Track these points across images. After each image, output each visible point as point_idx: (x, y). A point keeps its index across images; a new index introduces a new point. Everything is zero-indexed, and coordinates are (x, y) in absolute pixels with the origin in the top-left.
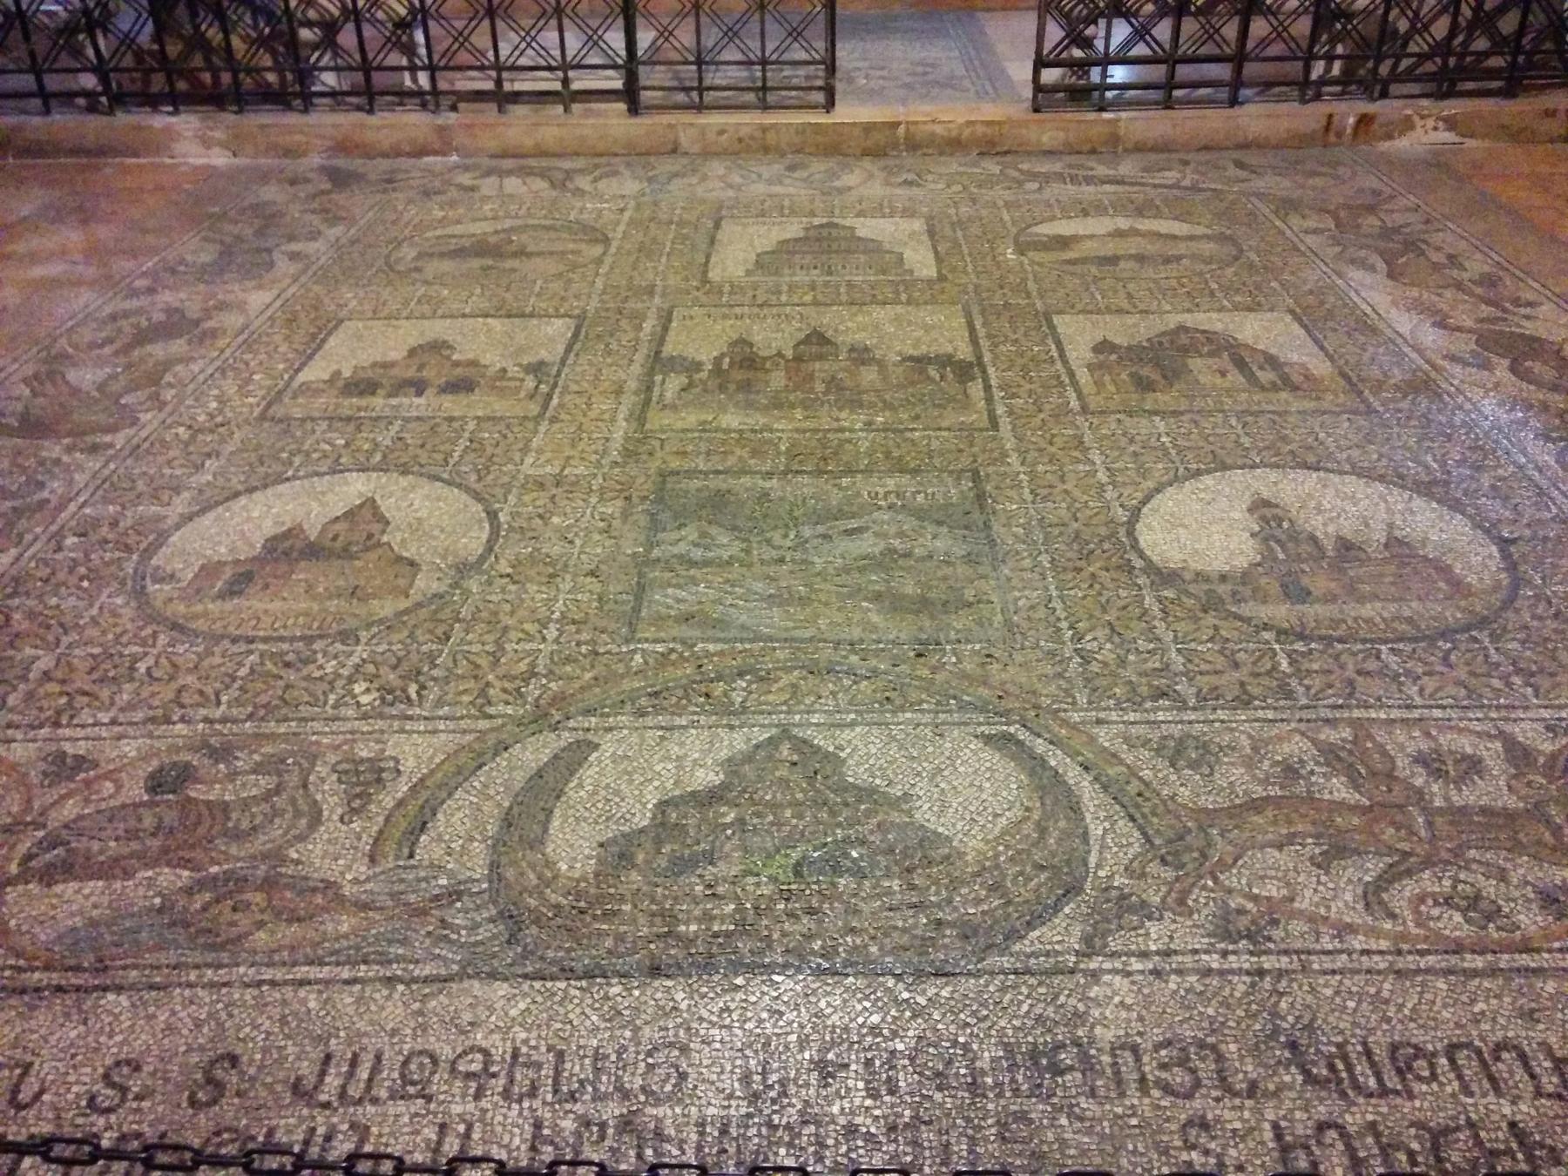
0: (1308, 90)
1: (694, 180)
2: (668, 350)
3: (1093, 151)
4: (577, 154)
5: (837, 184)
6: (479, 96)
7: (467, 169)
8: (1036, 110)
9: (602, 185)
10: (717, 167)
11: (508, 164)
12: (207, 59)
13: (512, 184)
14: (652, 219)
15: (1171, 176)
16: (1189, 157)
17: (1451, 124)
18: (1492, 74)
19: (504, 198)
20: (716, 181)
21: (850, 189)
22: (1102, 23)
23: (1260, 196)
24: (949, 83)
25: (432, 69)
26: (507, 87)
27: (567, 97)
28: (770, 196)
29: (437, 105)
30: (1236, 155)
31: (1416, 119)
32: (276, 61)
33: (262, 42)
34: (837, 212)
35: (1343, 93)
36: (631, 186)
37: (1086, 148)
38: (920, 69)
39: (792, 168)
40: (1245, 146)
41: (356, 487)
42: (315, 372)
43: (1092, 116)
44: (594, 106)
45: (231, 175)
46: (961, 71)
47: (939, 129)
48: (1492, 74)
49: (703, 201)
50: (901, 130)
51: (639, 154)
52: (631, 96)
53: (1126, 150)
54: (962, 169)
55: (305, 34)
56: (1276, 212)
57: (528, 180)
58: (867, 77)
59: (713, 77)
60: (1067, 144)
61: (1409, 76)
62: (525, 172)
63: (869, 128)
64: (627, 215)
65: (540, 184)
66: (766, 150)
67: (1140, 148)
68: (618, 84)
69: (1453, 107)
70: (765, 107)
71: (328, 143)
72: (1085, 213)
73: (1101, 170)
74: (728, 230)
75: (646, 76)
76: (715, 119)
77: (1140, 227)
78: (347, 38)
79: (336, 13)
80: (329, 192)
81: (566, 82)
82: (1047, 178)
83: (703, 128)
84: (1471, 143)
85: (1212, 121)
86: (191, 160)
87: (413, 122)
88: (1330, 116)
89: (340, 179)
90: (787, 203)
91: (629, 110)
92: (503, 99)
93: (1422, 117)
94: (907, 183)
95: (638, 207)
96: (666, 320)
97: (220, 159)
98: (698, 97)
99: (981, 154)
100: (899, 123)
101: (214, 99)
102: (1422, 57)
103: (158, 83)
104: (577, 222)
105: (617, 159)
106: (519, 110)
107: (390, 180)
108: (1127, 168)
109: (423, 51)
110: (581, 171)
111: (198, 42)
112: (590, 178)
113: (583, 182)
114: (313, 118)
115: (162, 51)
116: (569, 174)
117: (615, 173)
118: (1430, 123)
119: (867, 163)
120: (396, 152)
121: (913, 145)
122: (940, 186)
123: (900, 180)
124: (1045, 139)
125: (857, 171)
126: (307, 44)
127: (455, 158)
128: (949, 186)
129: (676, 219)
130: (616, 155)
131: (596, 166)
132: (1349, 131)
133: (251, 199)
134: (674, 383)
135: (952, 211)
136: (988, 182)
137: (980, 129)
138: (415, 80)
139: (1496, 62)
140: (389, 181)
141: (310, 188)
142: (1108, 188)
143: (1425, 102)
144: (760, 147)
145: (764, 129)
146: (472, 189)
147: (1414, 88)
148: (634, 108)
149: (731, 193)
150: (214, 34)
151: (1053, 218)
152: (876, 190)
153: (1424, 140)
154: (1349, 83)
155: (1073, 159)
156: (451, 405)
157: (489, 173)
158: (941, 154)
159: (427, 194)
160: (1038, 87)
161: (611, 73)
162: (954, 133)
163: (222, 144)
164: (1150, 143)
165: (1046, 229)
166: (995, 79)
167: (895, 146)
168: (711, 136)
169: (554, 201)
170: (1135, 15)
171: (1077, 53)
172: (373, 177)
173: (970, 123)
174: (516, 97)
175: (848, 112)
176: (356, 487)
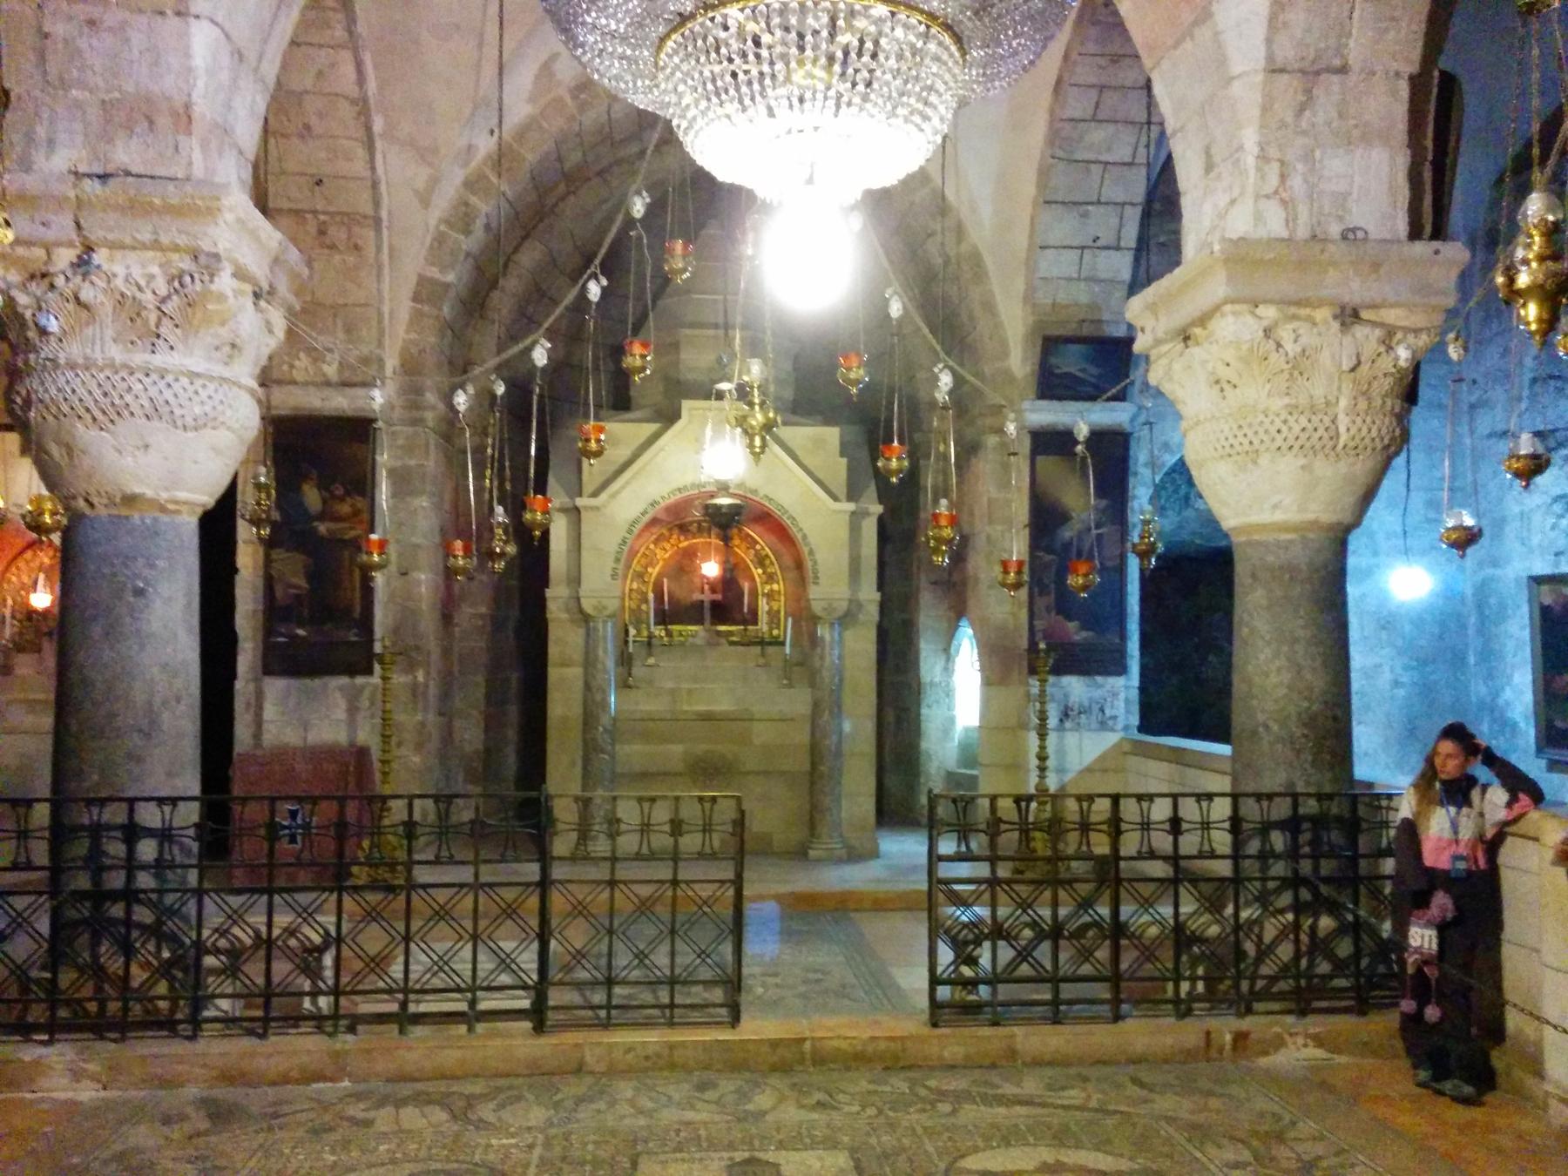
0: (1183, 1009)
1: (602, 1105)
3: (993, 1066)
4: (477, 1076)
5: (750, 1107)
6: (381, 1018)
7: (358, 1097)
8: (935, 1025)
9: (506, 1114)
10: (625, 1089)
11: (406, 1090)
12: (99, 989)
13: (411, 1117)
14: (564, 1159)
15: (1074, 1095)
16: (1084, 1071)
17: (1319, 1041)
18: (1339, 993)
19: (403, 1134)
21: (765, 1113)
22: (987, 945)
23: (1170, 1120)
24: (842, 992)
25: (336, 992)
26: (412, 1008)
27: (472, 1017)
28: (688, 1123)
29: (336, 1026)
30: (1131, 1069)
31: (1286, 1037)
32: (172, 988)
33: (165, 970)
34: (757, 1143)
35: (1212, 1008)
36: (537, 1115)
37: (987, 1062)
38: (811, 976)
39: (702, 1087)
40: (1136, 1061)
43: (987, 1031)
44: (500, 1025)
45: (96, 1111)
46: (851, 979)
47: (844, 1045)
48: (1339, 993)
49: (613, 1133)
50: (807, 1046)
51: (543, 1076)
52: (538, 1016)
53: (1024, 1064)
54: (871, 1087)
56: (1189, 1140)
57: (428, 1109)
58: (764, 985)
60: (967, 1057)
61: (1265, 995)
62: (422, 1100)
63: (775, 1044)
64: (537, 1152)
65: (440, 1115)
66: (672, 1066)
67: (1037, 1063)
68: (525, 1004)
70: (671, 1024)
71: (215, 1073)
72: (1006, 1142)
73: (1009, 1089)
75: (555, 997)
76: (622, 1037)
77: (1066, 1160)
78: (254, 970)
79: (248, 942)
80: (206, 1133)
81: (473, 1003)
82: (959, 1098)
83: (611, 1046)
84: (1342, 1059)
85: (1102, 1037)
86: (55, 1095)
87: (303, 1046)
88: (1208, 1033)
89: (220, 1115)
90: (702, 1132)
91: (534, 1029)
92: (405, 1020)
93: (1291, 1035)
94: (820, 1105)
95: (548, 1145)
97: (87, 1093)
98: (608, 1017)
99: (886, 1069)
100: (804, 1040)
102: (1273, 979)
103: (37, 1014)
104: (484, 1164)
105: (521, 1080)
106: (418, 1031)
107: (274, 1116)
108: (1031, 1085)
109: (329, 974)
110: (484, 1097)
111: (98, 971)
112: (492, 1105)
113: (486, 1111)
114: (200, 1046)
115: (54, 981)
116: (471, 1101)
117: (519, 1098)
118: (1300, 1040)
119: (774, 1080)
120: (285, 1080)
121: (821, 1059)
122: (856, 1108)
123: (812, 1100)
124: (946, 1054)
125: (768, 1091)
126: (213, 971)
127: (346, 1083)
128: (863, 1108)
129: (589, 1157)
130: (518, 1076)
131: (499, 1090)
132: (1228, 1047)
133: (118, 1147)
135: (873, 1141)
136: (899, 1104)
137: (882, 1045)
138: (314, 1003)
139: (1341, 983)
140: (276, 1116)
141: (187, 1127)
142: (1020, 1110)
143: (1290, 1019)
144: (668, 1063)
145: (672, 1047)
146: (368, 1123)
147: (1276, 1006)
148: (540, 1028)
149: (642, 1121)
150: (115, 965)
151: (976, 1150)
152: (792, 1114)
153: (1297, 1055)
154: (1213, 999)
155: (977, 1074)
157: (382, 1103)
158: (848, 1069)
159: (316, 1132)
160: (935, 1004)
161: (521, 993)
162: (859, 1048)
163: (94, 1078)
164: (1047, 1057)
166: (885, 992)
167: (802, 1061)
168: (618, 1054)
169: (457, 1136)
170: (1016, 938)
171: (967, 971)
172: (254, 1109)
173: (873, 1039)
174: (419, 1019)
175: (757, 1027)
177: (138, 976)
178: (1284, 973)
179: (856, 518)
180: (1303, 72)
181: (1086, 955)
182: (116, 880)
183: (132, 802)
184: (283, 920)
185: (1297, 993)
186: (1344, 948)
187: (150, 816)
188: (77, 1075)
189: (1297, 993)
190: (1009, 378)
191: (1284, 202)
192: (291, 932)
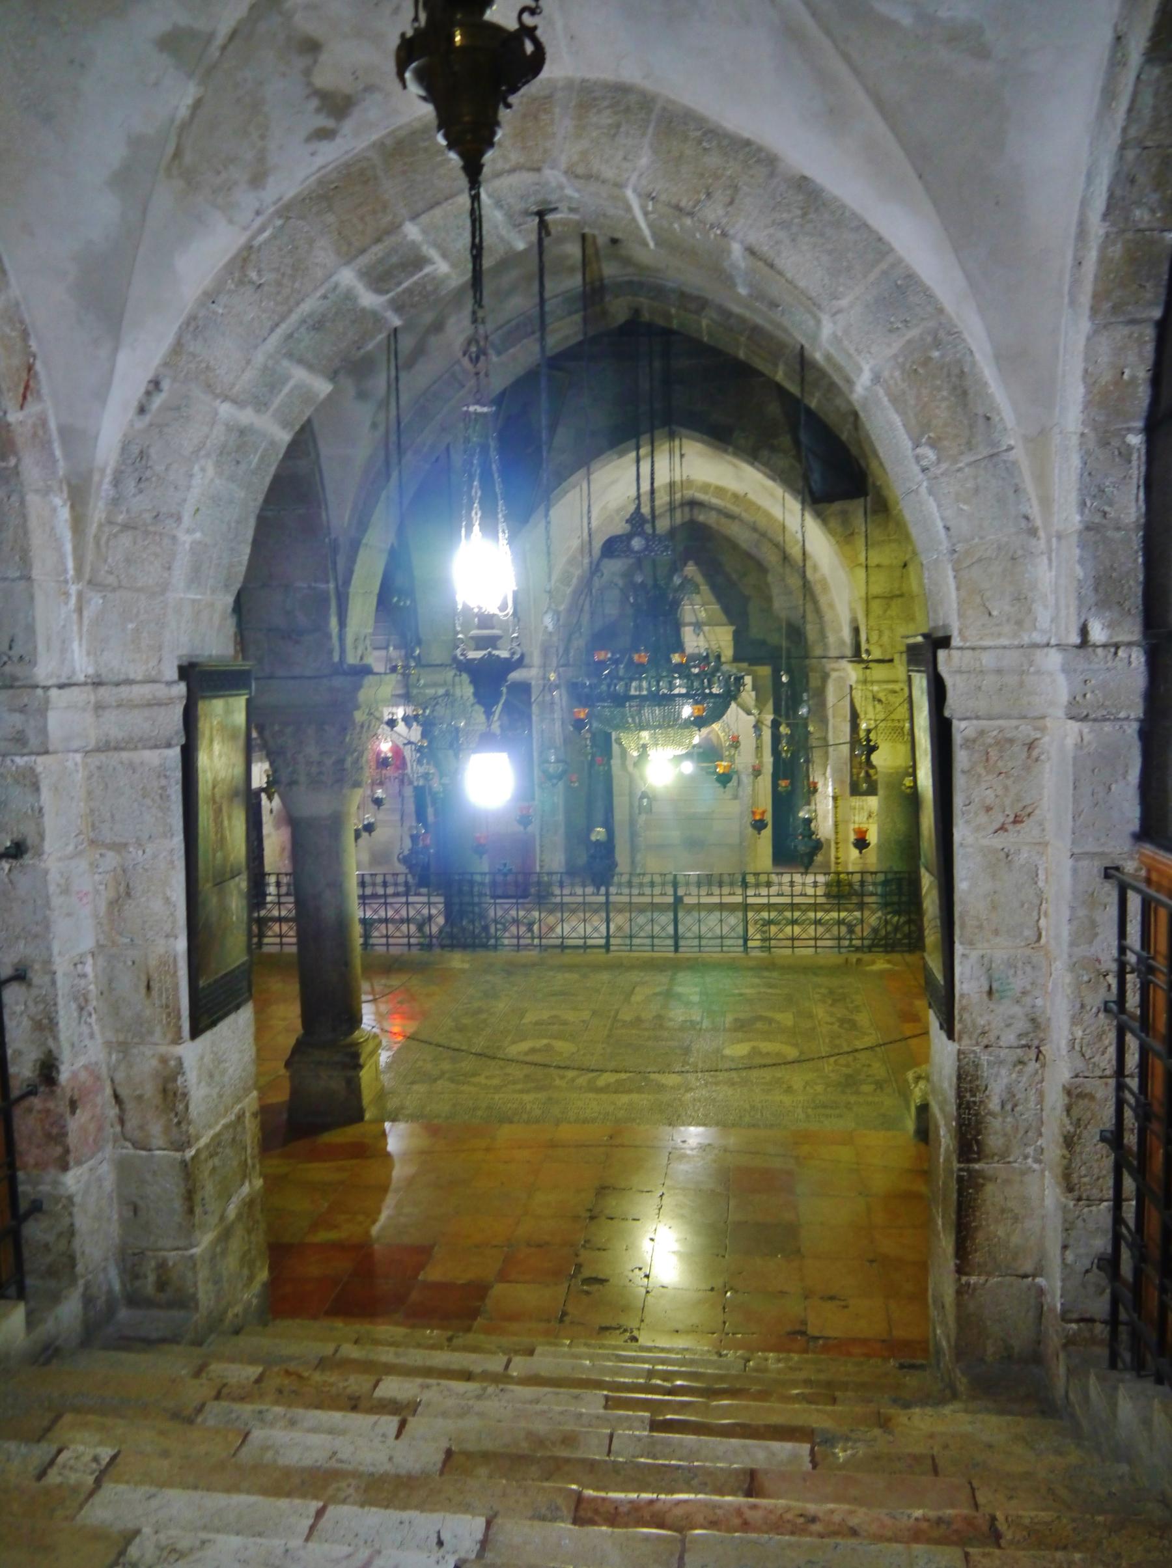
2: (619, 1017)
3: (767, 969)
17: (889, 962)
20: (635, 976)
25: (540, 938)
41: (545, 1041)
42: (524, 1021)
55: (499, 926)
59: (636, 941)
61: (877, 946)
69: (888, 957)
73: (766, 974)
74: (637, 989)
75: (612, 941)
96: (617, 1012)
101: (465, 947)
102: (881, 940)
108: (775, 974)
134: (619, 1024)
139: (906, 941)
145: (653, 959)
156: (562, 1027)
165: (737, 991)
176: (545, 1041)
177: (477, 931)
178: (886, 937)
179: (757, 727)
180: (885, 598)
181: (804, 931)
182: (466, 899)
183: (472, 874)
184: (522, 913)
185: (886, 946)
186: (906, 929)
187: (478, 878)
188: (463, 961)
189: (886, 946)
190: (843, 643)
191: (881, 646)
192: (502, 917)
